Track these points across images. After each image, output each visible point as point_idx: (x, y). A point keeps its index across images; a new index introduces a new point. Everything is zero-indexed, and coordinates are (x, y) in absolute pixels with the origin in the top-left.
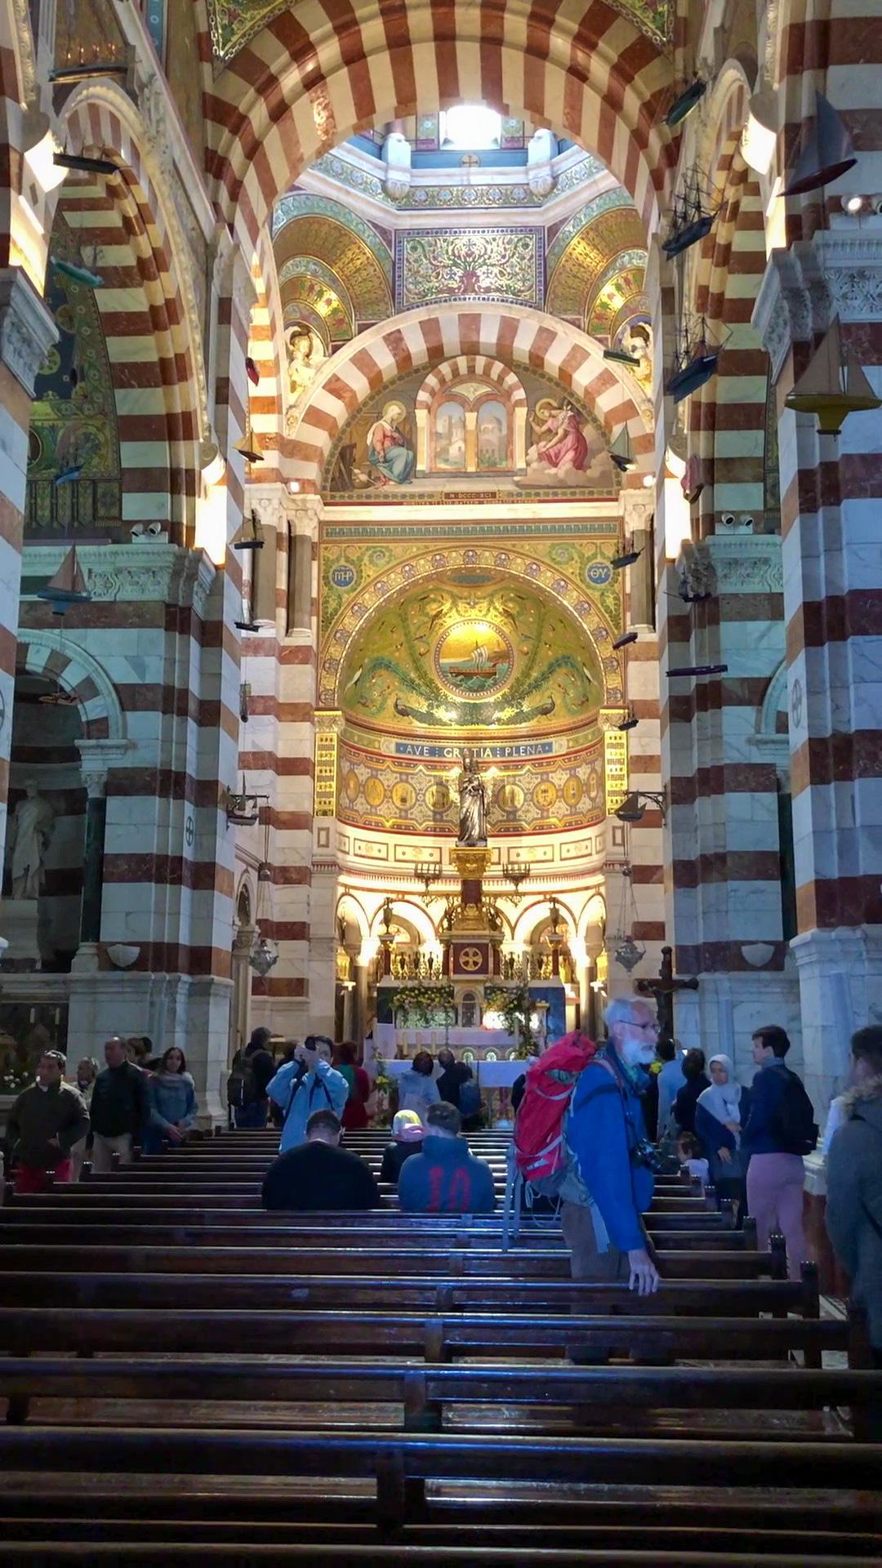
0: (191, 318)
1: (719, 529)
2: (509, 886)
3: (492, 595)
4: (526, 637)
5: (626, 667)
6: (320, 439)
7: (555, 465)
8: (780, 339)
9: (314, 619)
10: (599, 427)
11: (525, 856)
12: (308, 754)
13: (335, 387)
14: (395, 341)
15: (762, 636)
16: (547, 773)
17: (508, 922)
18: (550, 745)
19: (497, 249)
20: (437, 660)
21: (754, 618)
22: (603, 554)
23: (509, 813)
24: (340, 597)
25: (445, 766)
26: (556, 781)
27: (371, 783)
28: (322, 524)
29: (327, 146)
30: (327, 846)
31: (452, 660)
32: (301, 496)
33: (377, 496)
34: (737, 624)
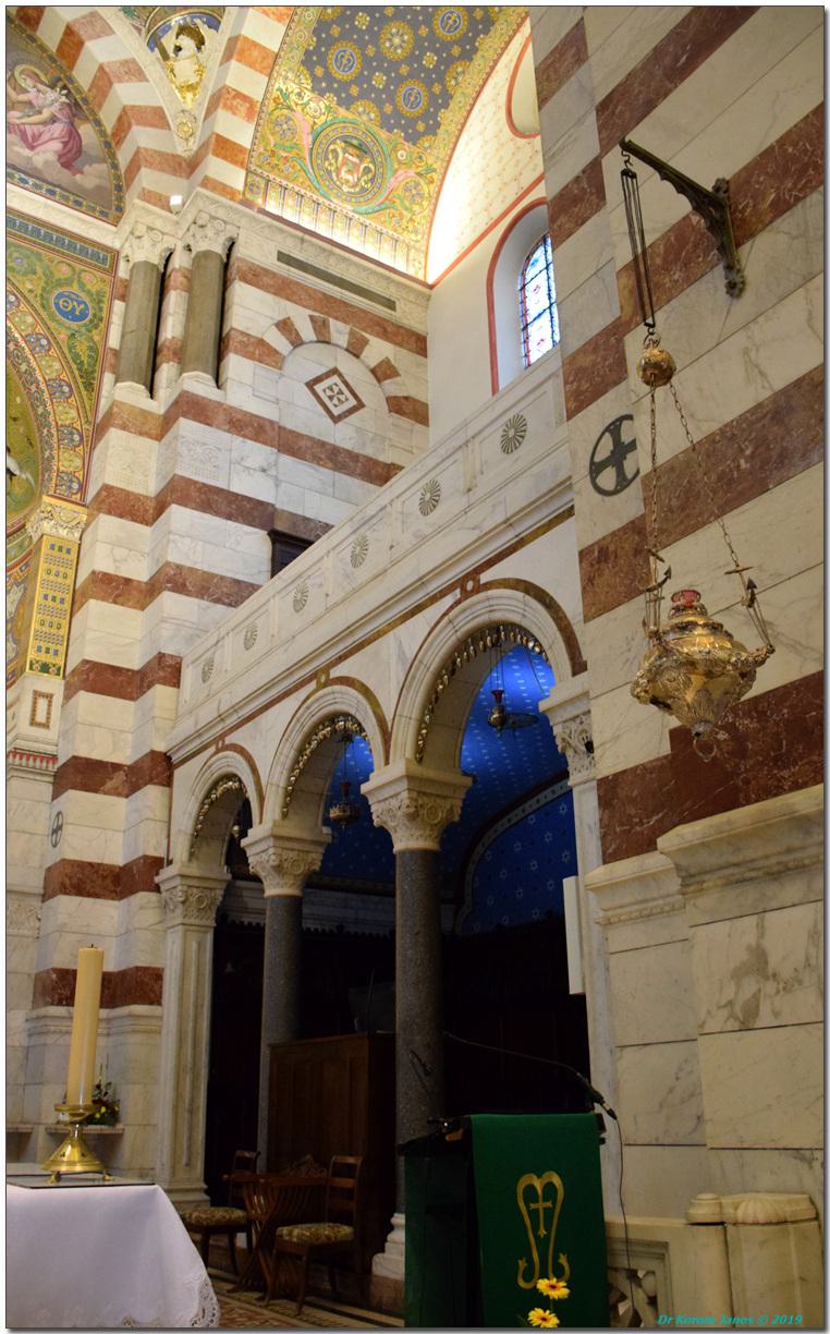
5: (92, 448)
7: (32, 148)
10: (102, 133)
22: (82, 286)
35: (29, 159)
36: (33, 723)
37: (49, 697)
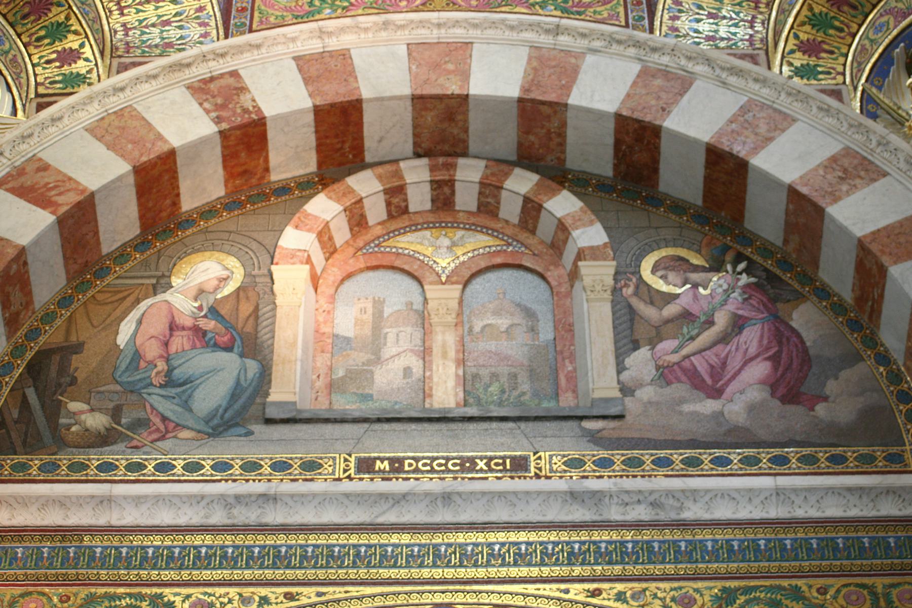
7: (716, 393)
10: (838, 308)
35: (718, 416)
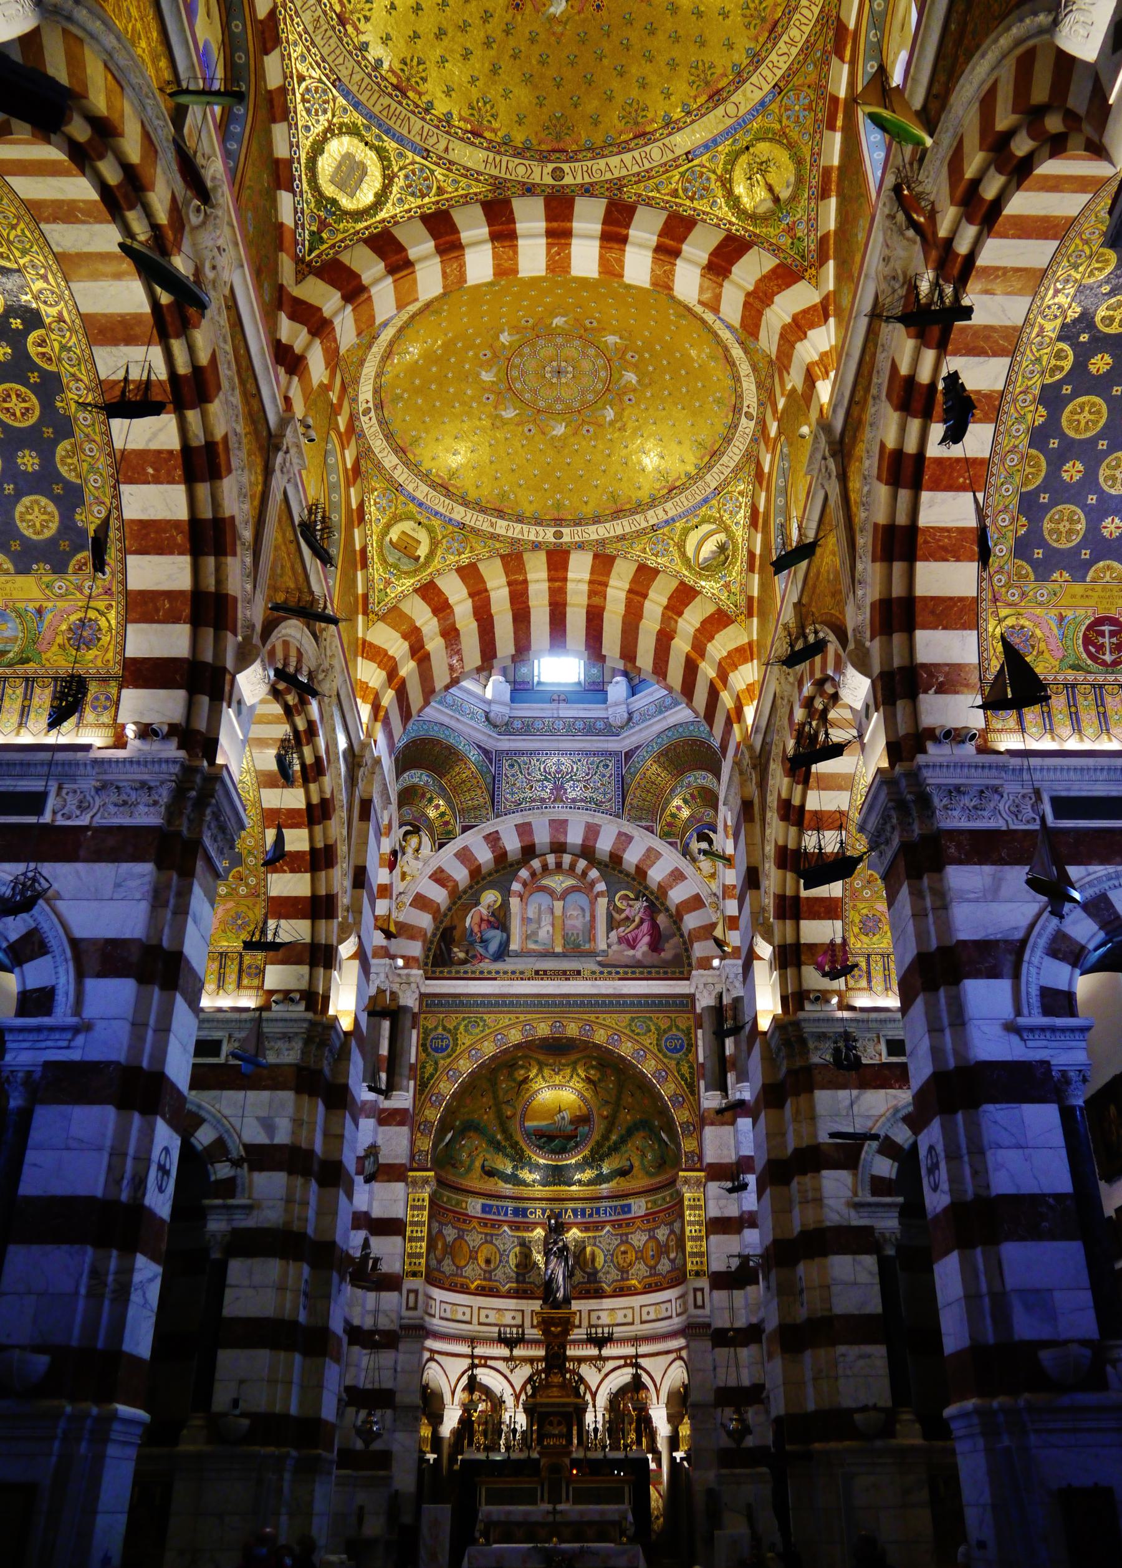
0: (340, 815)
1: (808, 1006)
2: (593, 1351)
3: (575, 1063)
4: (607, 1102)
6: (424, 921)
7: (633, 948)
8: (888, 842)
9: (412, 1083)
10: (671, 916)
11: (605, 1319)
12: (400, 1215)
13: (440, 877)
14: (493, 839)
15: (852, 1105)
16: (627, 1235)
17: (588, 1387)
18: (629, 1206)
19: (581, 772)
20: (522, 1125)
21: (844, 1086)
22: (678, 1028)
23: (589, 1274)
24: (436, 1063)
25: (530, 1227)
26: (635, 1243)
27: (458, 1243)
28: (422, 996)
29: (455, 682)
30: (415, 1308)
31: (535, 1123)
32: (406, 971)
33: (473, 972)
34: (828, 1092)
36: (696, 1306)
37: (702, 1290)
